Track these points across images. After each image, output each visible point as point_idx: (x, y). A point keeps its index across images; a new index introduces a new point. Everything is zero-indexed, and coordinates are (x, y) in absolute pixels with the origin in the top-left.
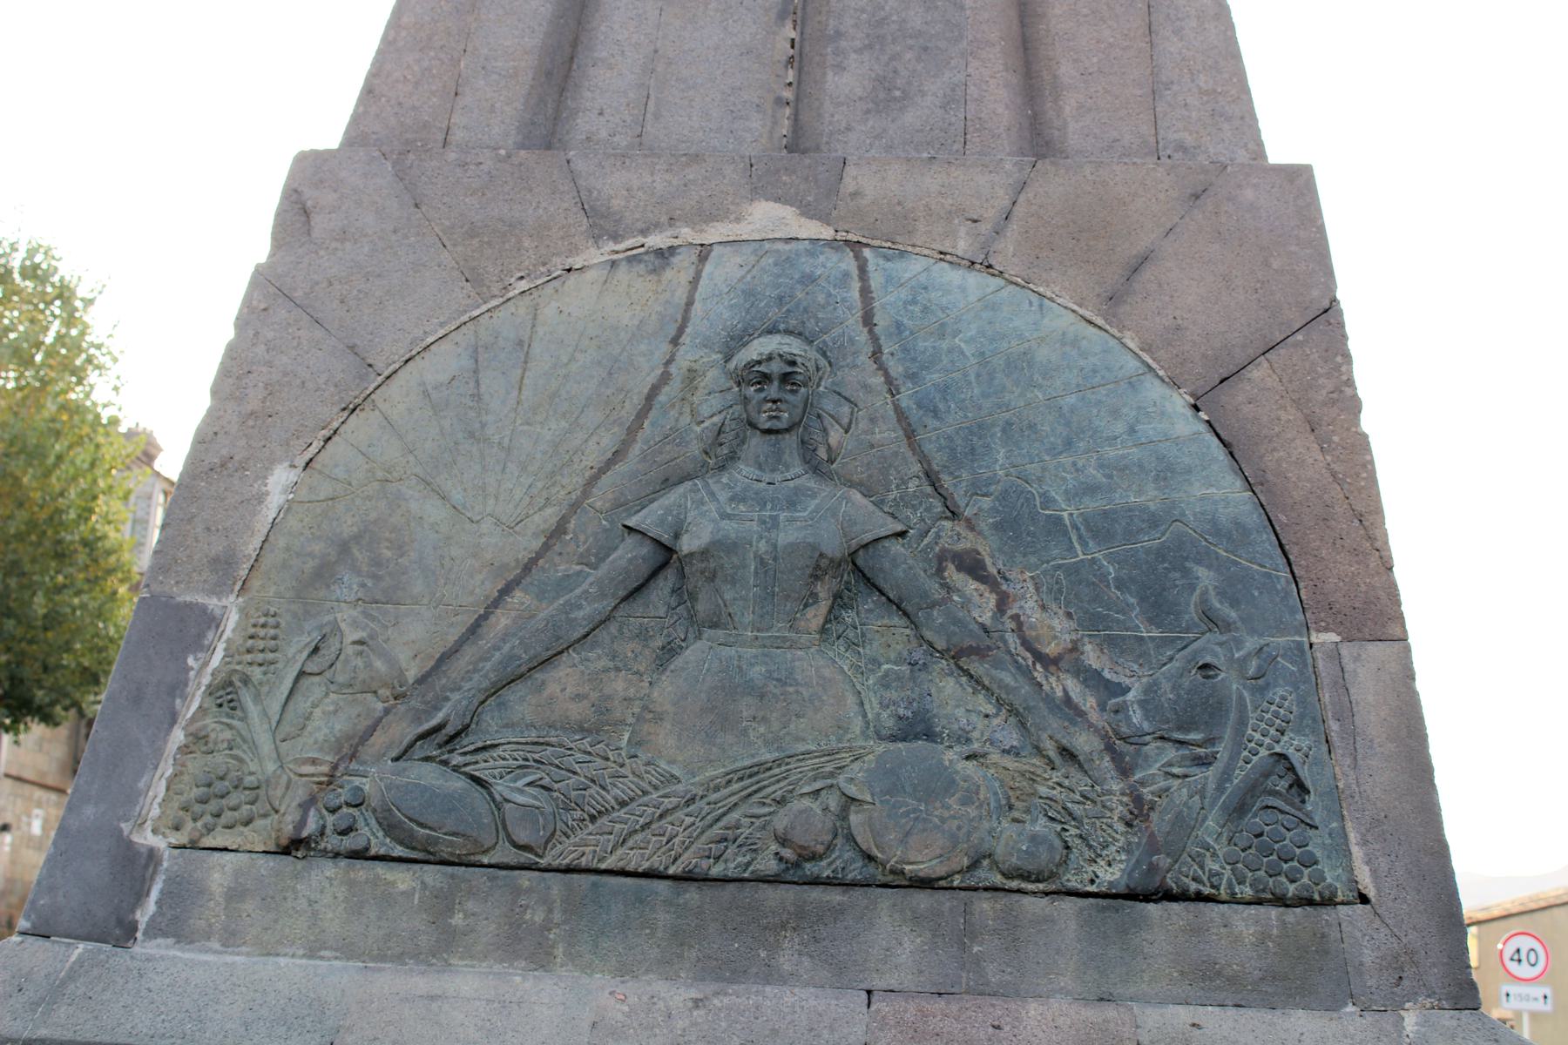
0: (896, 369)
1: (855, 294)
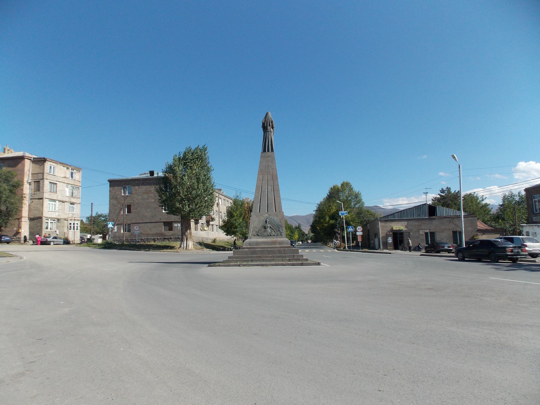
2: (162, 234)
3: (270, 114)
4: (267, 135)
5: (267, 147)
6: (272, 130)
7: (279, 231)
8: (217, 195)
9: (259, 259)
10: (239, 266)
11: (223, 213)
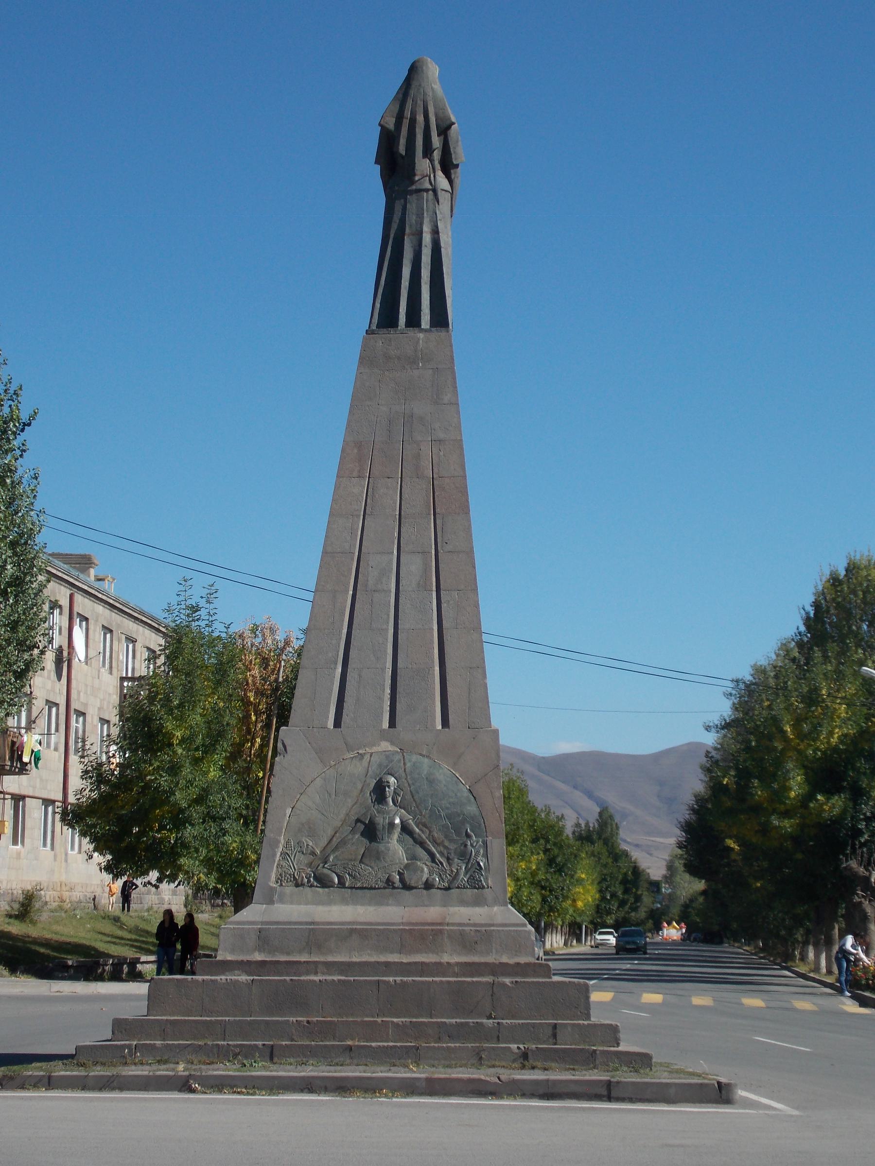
0: (410, 782)
3: (433, 71)
4: (411, 218)
6: (442, 182)
7: (464, 855)
8: (62, 594)
9: (321, 1041)
10: (184, 1086)
11: (93, 719)
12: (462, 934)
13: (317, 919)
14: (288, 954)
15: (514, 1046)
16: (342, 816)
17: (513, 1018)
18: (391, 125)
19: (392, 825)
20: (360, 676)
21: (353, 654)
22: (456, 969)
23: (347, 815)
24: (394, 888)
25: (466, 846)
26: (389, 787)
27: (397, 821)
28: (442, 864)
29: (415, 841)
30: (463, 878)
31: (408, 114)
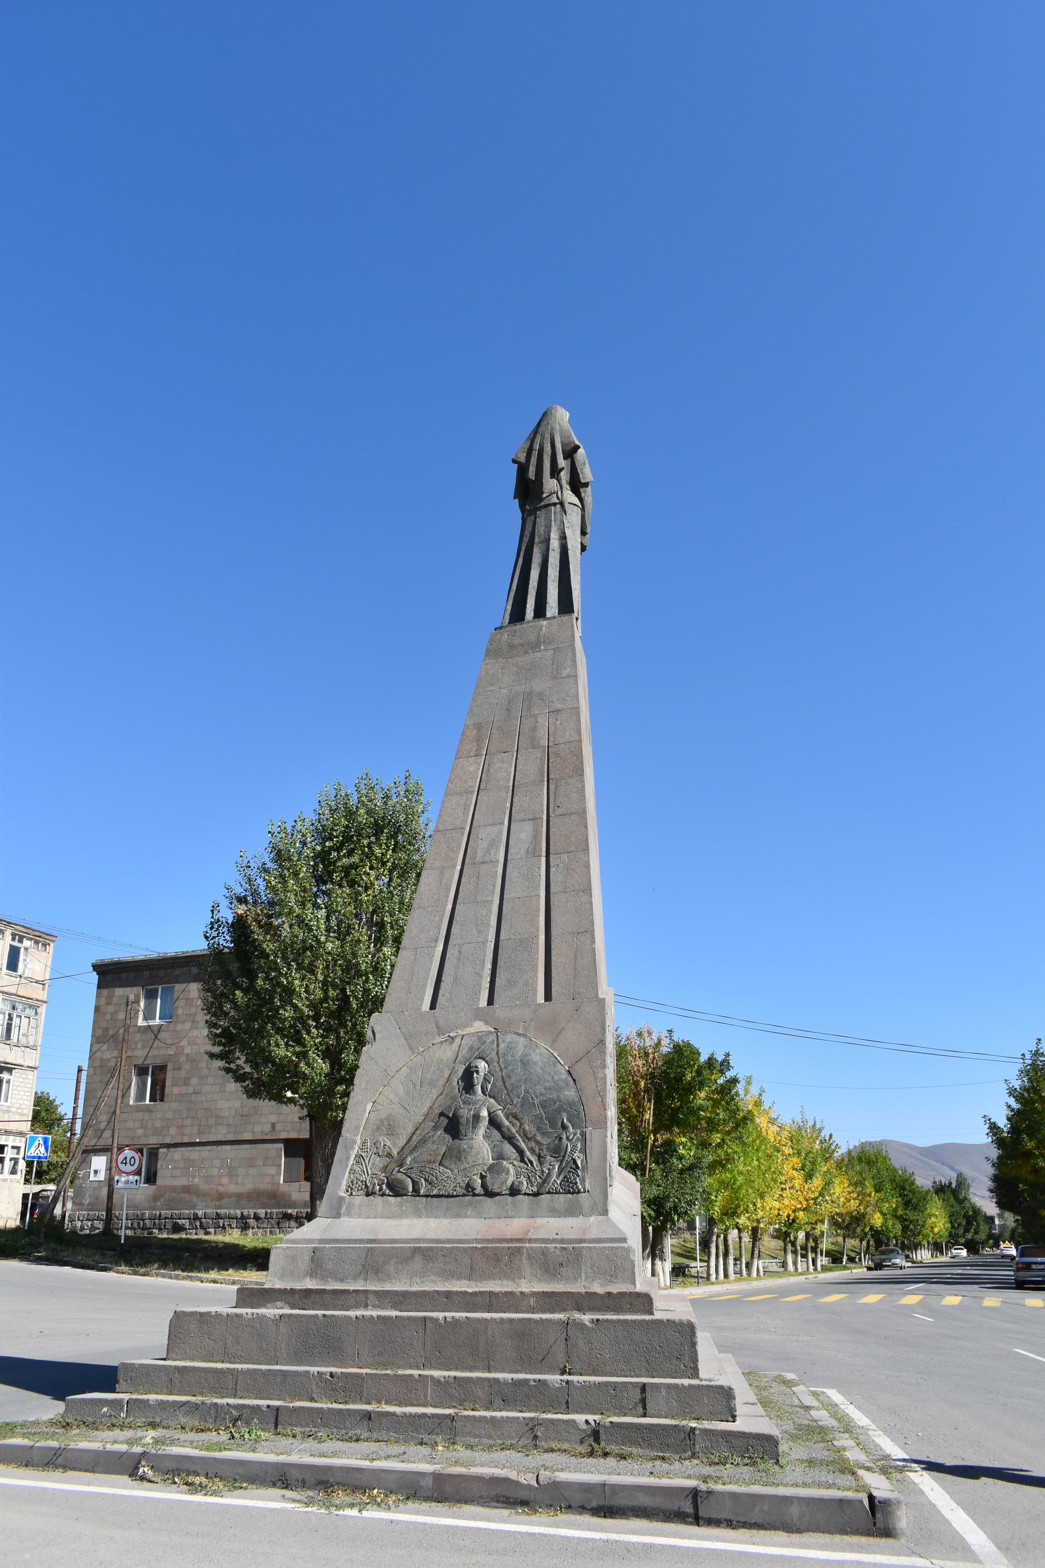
0: (502, 1066)
1: (495, 1046)
2: (274, 1197)
4: (540, 529)
5: (531, 594)
6: (570, 497)
7: (557, 1151)
12: (544, 1253)
13: (381, 1237)
14: (342, 1280)
15: (580, 1418)
16: (425, 1109)
17: (595, 1373)
18: (522, 458)
19: (477, 1118)
20: (460, 952)
21: (454, 930)
22: (532, 1301)
23: (431, 1108)
24: (475, 1195)
25: (560, 1139)
26: (477, 1072)
27: (484, 1113)
28: (531, 1163)
29: (503, 1137)
30: (556, 1180)
31: (537, 447)
